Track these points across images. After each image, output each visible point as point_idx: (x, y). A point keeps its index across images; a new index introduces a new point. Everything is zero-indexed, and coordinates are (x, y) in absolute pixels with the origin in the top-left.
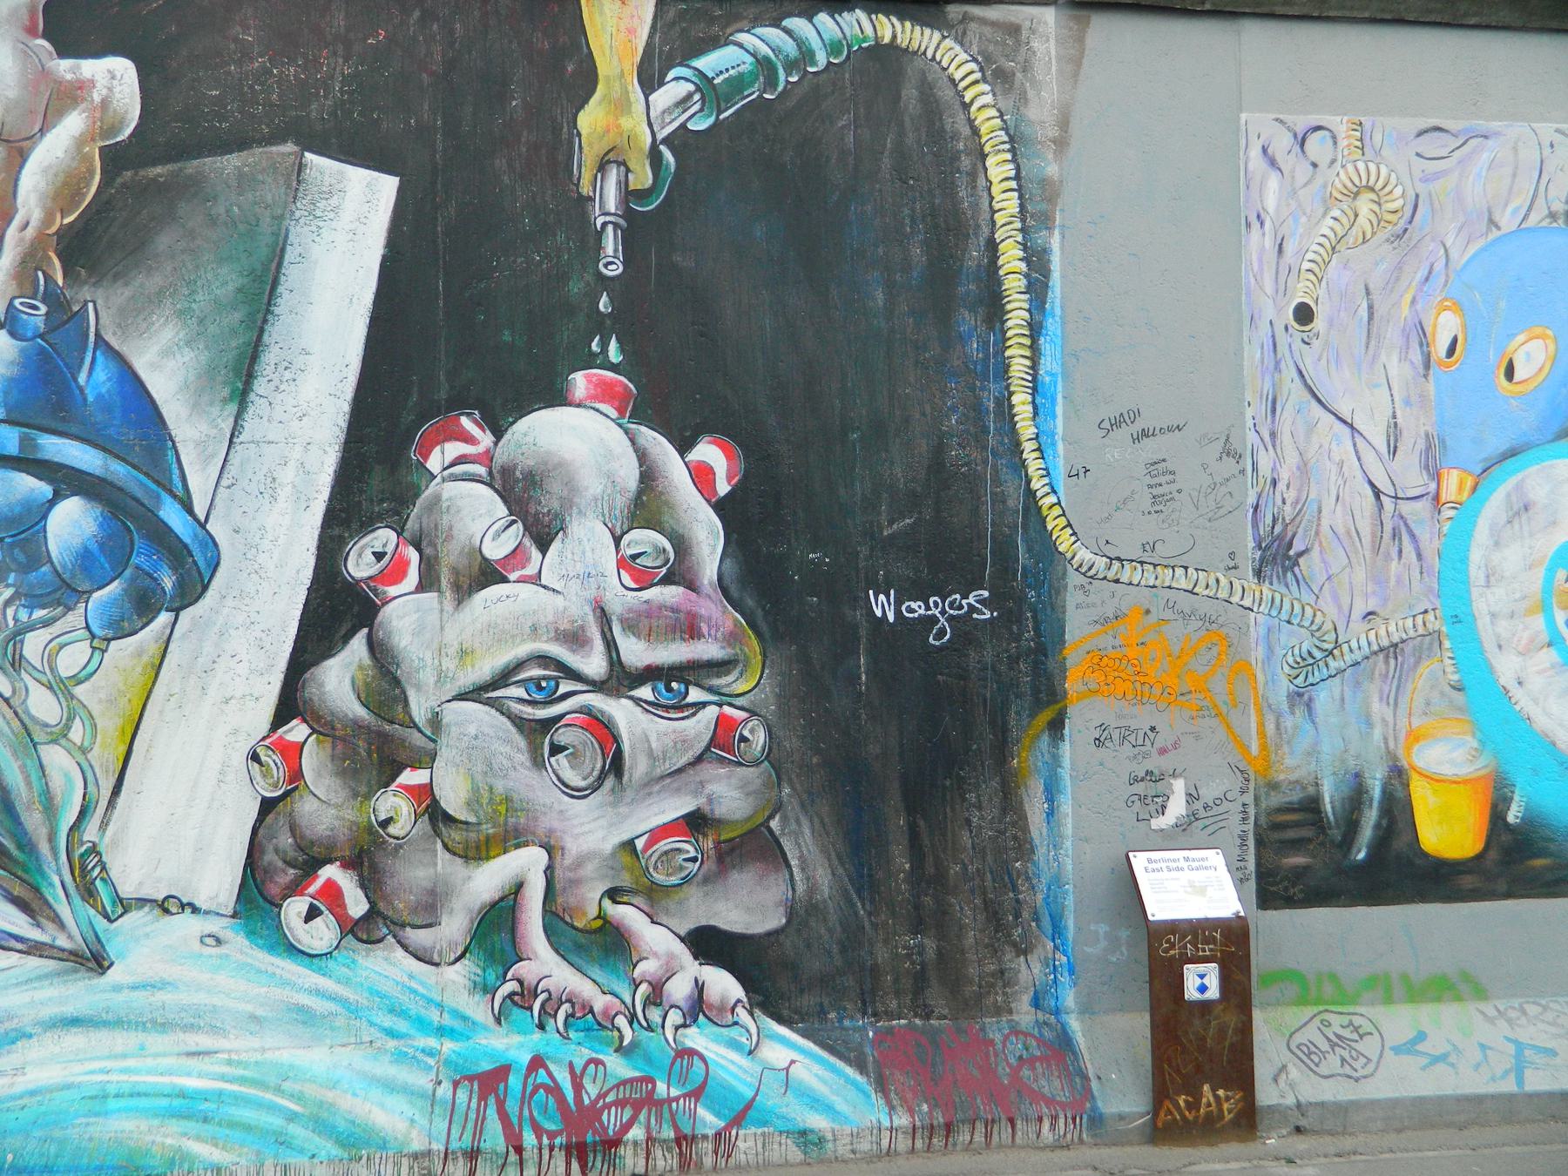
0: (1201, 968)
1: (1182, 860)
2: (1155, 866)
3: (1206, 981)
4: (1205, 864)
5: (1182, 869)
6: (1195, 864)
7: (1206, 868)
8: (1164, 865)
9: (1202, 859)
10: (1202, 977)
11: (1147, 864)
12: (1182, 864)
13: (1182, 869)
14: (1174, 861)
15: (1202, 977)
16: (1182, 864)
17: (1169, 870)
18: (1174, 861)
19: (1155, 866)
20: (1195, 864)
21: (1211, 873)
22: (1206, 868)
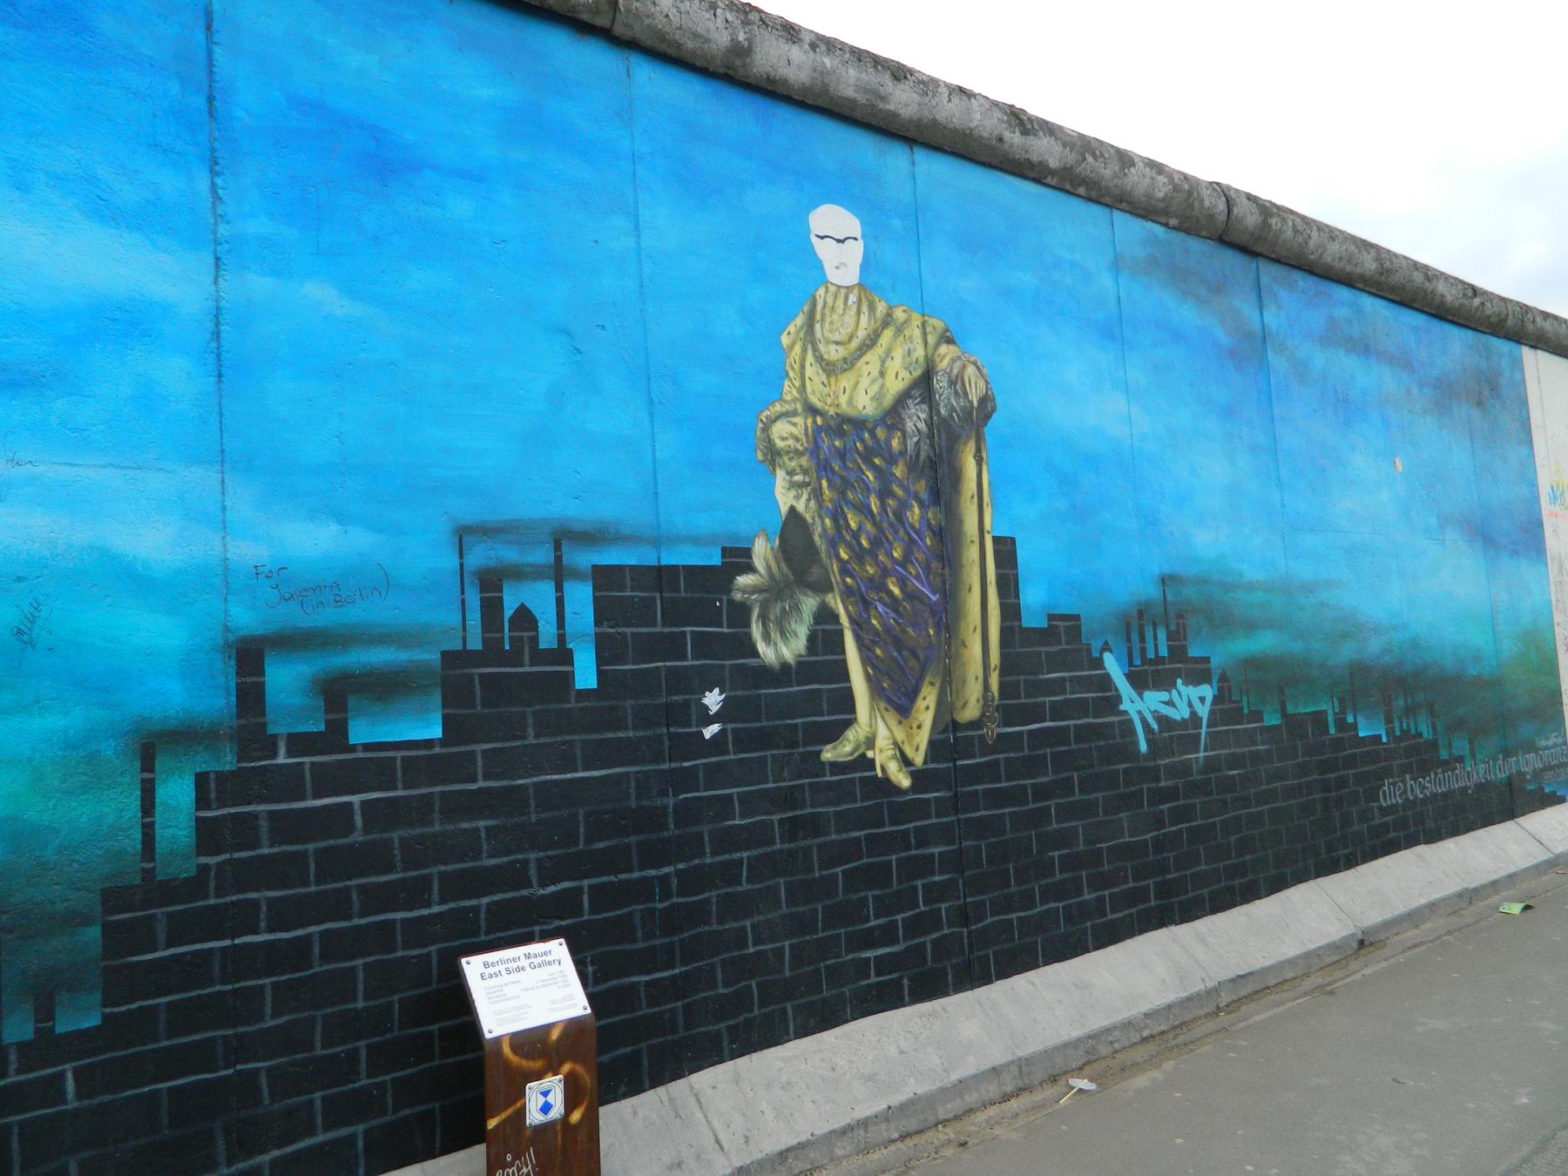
1: (523, 958)
2: (492, 970)
3: (550, 1099)
4: (548, 958)
5: (523, 969)
7: (549, 963)
8: (502, 968)
9: (545, 953)
11: (483, 970)
12: (524, 962)
13: (523, 969)
14: (514, 960)
15: (545, 1094)
16: (524, 962)
17: (509, 972)
18: (514, 960)
19: (492, 970)
21: (555, 967)
22: (549, 963)
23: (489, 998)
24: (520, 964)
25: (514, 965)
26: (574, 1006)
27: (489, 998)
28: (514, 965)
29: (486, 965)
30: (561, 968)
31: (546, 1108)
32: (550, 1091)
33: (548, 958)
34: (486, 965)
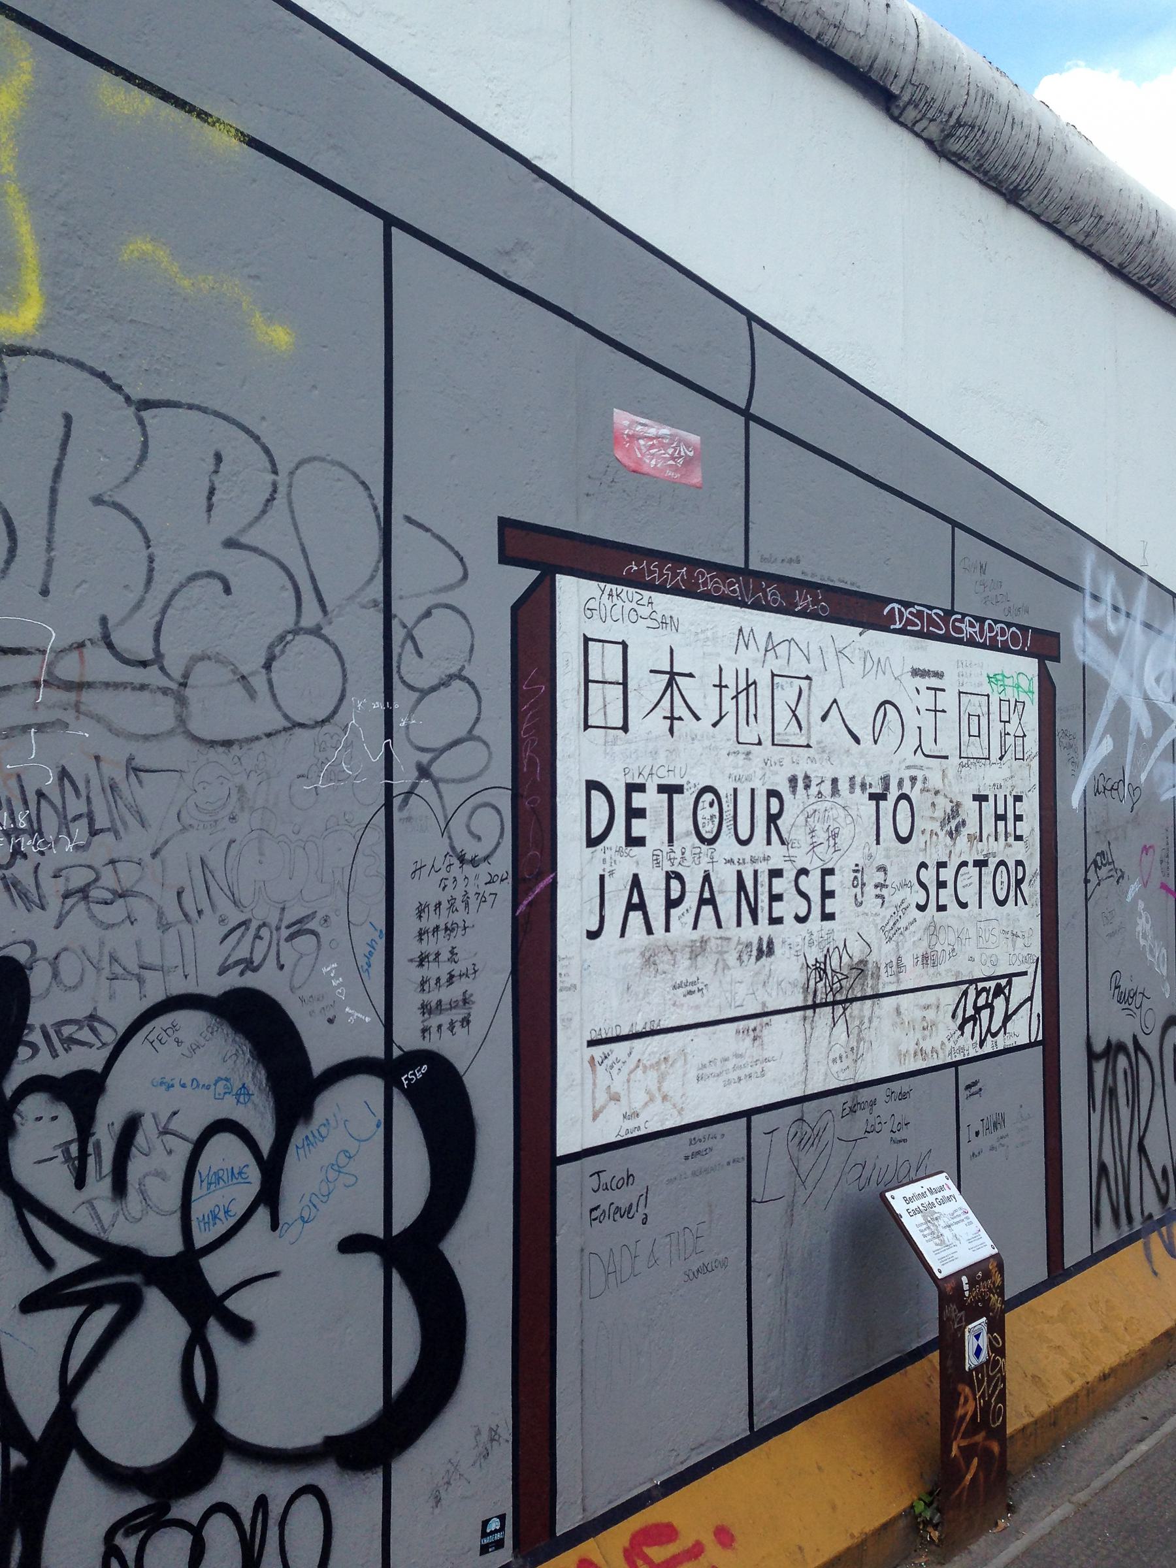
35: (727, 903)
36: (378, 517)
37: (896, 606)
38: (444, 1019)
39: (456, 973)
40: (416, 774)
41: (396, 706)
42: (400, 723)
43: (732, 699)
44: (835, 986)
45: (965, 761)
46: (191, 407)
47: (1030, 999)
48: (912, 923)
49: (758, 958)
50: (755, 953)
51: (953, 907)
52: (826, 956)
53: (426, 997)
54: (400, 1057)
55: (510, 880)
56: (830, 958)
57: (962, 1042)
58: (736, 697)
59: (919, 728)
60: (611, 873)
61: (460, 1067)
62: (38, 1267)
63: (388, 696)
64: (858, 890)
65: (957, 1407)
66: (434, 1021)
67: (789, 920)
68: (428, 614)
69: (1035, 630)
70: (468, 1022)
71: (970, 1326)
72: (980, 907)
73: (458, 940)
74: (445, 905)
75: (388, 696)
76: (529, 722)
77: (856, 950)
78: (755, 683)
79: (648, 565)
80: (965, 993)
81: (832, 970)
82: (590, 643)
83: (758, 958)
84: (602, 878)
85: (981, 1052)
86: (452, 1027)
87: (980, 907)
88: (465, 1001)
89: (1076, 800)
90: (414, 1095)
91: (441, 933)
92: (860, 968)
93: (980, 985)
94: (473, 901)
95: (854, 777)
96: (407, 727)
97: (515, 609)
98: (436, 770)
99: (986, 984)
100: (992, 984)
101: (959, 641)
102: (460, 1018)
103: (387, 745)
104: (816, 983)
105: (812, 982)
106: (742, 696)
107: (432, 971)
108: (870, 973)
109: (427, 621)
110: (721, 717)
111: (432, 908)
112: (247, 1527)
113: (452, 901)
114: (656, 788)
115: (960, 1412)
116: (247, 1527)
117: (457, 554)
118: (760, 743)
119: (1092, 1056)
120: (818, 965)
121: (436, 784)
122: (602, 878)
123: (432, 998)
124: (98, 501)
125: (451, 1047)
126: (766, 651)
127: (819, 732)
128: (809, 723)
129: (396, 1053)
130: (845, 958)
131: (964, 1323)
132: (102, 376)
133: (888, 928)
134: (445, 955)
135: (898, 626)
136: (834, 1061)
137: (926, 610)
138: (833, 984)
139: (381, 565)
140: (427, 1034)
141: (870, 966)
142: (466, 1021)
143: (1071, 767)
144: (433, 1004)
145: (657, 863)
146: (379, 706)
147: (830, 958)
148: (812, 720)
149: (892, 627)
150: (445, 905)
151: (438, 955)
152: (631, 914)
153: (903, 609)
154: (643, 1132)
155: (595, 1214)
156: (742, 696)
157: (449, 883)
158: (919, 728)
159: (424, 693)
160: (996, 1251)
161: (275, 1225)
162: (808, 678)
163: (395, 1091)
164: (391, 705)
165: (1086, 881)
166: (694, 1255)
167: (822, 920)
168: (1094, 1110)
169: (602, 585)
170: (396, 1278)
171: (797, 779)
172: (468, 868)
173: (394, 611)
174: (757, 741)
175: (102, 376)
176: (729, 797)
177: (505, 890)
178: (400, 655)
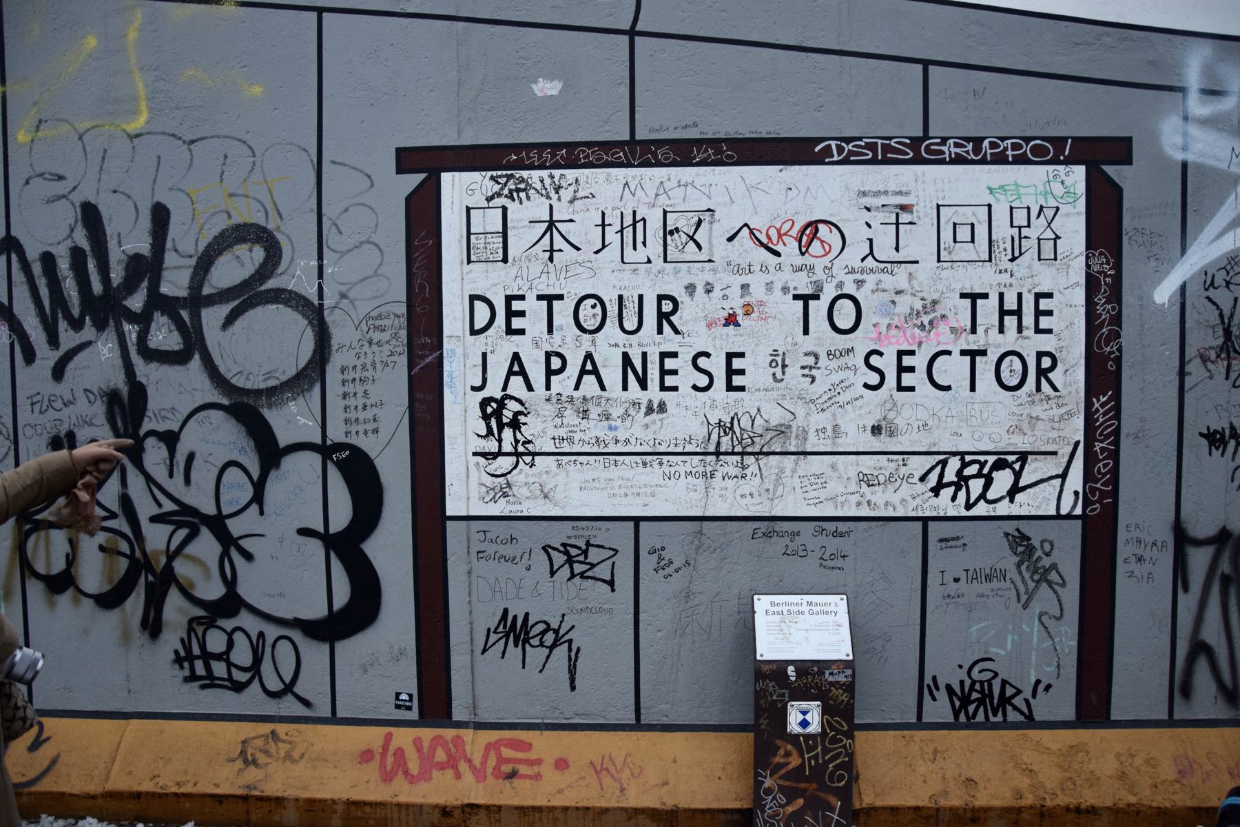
0: (804, 705)
2: (776, 609)
3: (808, 717)
4: (826, 609)
5: (803, 613)
6: (816, 609)
8: (785, 609)
9: (825, 604)
10: (804, 713)
11: (768, 607)
12: (805, 608)
13: (803, 613)
15: (804, 713)
16: (805, 608)
19: (776, 609)
20: (816, 609)
21: (831, 618)
23: (768, 630)
24: (801, 609)
25: (796, 609)
26: (838, 651)
27: (768, 630)
28: (796, 609)
29: (772, 604)
30: (836, 619)
31: (804, 724)
32: (808, 712)
33: (826, 609)
34: (772, 604)
35: (612, 375)
36: (313, 165)
37: (833, 143)
38: (361, 428)
39: (369, 404)
40: (339, 297)
41: (325, 262)
42: (328, 271)
43: (617, 233)
44: (744, 442)
45: (945, 265)
46: (212, 137)
47: (1063, 476)
48: (856, 399)
49: (647, 414)
50: (643, 409)
51: (924, 388)
52: (733, 419)
53: (348, 415)
54: (330, 445)
55: (406, 354)
56: (739, 421)
57: (935, 502)
58: (621, 231)
59: (871, 240)
60: (493, 352)
61: (372, 455)
62: (156, 506)
63: (320, 256)
64: (778, 370)
65: (775, 755)
66: (354, 428)
67: (685, 389)
68: (346, 210)
69: (1074, 139)
70: (377, 432)
71: (793, 703)
72: (973, 389)
73: (369, 387)
74: (359, 367)
75: (320, 256)
76: (420, 262)
77: (776, 416)
78: (644, 220)
79: (528, 155)
80: (944, 463)
81: (741, 429)
82: (472, 211)
83: (647, 414)
84: (484, 355)
85: (964, 513)
86: (366, 433)
87: (973, 389)
88: (375, 420)
89: (1164, 293)
90: (340, 465)
91: (357, 382)
92: (782, 431)
93: (968, 458)
94: (379, 366)
95: (772, 282)
96: (333, 272)
97: (408, 199)
98: (351, 294)
99: (982, 458)
100: (991, 459)
101: (942, 162)
102: (371, 429)
103: (319, 283)
104: (719, 437)
105: (714, 437)
106: (628, 233)
107: (352, 402)
108: (794, 435)
109: (345, 214)
110: (604, 246)
111: (350, 368)
112: (255, 642)
113: (364, 367)
114: (535, 297)
115: (777, 759)
116: (255, 642)
117: (366, 175)
118: (649, 261)
119: (1182, 538)
120: (722, 424)
121: (352, 302)
122: (484, 355)
123: (353, 416)
124: (171, 189)
125: (367, 444)
126: (657, 195)
127: (721, 251)
128: (710, 243)
129: (329, 442)
130: (759, 421)
131: (787, 699)
132: (173, 135)
133: (820, 401)
134: (360, 394)
135: (836, 158)
136: (743, 496)
137: (880, 142)
138: (742, 439)
139: (316, 190)
140: (349, 435)
141: (794, 429)
142: (376, 431)
143: (1153, 263)
144: (353, 420)
145: (536, 344)
146: (314, 263)
147: (739, 421)
148: (715, 241)
149: (827, 160)
150: (359, 367)
151: (355, 394)
152: (512, 378)
153: (843, 144)
154: (525, 514)
155: (480, 555)
156: (628, 233)
157: (362, 356)
158: (871, 240)
159: (343, 254)
160: (851, 658)
161: (262, 513)
162: (709, 210)
163: (329, 462)
164: (322, 261)
165: (1182, 374)
166: (577, 599)
167: (727, 391)
168: (1186, 589)
169: (484, 173)
170: (333, 555)
171: (695, 287)
172: (375, 348)
173: (324, 212)
174: (646, 260)
175: (173, 135)
176: (613, 301)
177: (403, 360)
178: (327, 235)
